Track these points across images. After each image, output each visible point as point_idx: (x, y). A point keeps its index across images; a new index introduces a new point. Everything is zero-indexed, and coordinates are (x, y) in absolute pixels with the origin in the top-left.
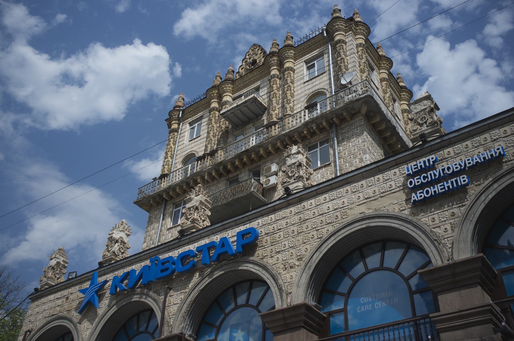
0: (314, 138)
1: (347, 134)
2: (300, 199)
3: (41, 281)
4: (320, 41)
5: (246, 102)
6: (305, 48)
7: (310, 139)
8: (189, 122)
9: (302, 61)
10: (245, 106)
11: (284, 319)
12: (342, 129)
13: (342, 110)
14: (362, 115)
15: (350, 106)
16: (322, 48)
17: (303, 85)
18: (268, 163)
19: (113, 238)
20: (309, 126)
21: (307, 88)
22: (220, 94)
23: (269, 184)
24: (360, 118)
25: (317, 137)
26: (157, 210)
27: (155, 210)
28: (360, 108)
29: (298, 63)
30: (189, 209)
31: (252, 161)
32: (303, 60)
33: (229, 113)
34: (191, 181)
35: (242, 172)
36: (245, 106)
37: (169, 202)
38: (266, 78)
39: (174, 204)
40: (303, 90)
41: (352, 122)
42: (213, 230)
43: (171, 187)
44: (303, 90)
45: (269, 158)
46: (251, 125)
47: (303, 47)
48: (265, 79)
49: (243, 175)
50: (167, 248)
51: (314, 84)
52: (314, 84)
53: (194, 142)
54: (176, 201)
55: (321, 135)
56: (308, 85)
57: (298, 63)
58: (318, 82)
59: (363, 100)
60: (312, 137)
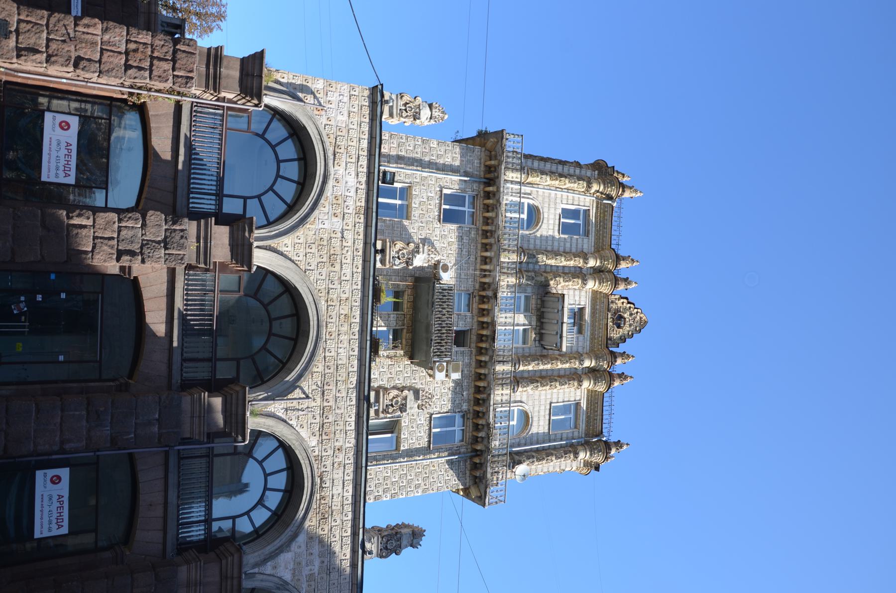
0: (471, 424)
1: (457, 468)
2: (355, 565)
3: (402, 97)
4: (593, 426)
5: (561, 337)
8: (591, 211)
9: (582, 399)
10: (557, 333)
11: (232, 578)
12: (466, 461)
13: (484, 472)
15: (484, 481)
16: (584, 428)
17: (548, 402)
18: (468, 359)
19: (416, 254)
20: (486, 428)
21: (543, 408)
22: (602, 271)
23: (436, 371)
24: (468, 484)
25: (471, 427)
26: (480, 163)
27: (480, 160)
28: (478, 487)
29: (583, 394)
30: (405, 398)
31: (481, 338)
32: (582, 401)
33: (560, 308)
34: (492, 240)
35: (473, 319)
36: (557, 333)
37: (482, 187)
38: (588, 345)
39: (477, 195)
40: (543, 402)
41: (468, 474)
42: (360, 453)
43: (498, 204)
44: (543, 402)
45: (474, 360)
46: (534, 323)
47: (599, 403)
48: (588, 342)
49: (468, 320)
50: (363, 381)
51: (542, 418)
53: (554, 224)
55: (471, 434)
56: (545, 409)
57: (583, 394)
60: (474, 423)
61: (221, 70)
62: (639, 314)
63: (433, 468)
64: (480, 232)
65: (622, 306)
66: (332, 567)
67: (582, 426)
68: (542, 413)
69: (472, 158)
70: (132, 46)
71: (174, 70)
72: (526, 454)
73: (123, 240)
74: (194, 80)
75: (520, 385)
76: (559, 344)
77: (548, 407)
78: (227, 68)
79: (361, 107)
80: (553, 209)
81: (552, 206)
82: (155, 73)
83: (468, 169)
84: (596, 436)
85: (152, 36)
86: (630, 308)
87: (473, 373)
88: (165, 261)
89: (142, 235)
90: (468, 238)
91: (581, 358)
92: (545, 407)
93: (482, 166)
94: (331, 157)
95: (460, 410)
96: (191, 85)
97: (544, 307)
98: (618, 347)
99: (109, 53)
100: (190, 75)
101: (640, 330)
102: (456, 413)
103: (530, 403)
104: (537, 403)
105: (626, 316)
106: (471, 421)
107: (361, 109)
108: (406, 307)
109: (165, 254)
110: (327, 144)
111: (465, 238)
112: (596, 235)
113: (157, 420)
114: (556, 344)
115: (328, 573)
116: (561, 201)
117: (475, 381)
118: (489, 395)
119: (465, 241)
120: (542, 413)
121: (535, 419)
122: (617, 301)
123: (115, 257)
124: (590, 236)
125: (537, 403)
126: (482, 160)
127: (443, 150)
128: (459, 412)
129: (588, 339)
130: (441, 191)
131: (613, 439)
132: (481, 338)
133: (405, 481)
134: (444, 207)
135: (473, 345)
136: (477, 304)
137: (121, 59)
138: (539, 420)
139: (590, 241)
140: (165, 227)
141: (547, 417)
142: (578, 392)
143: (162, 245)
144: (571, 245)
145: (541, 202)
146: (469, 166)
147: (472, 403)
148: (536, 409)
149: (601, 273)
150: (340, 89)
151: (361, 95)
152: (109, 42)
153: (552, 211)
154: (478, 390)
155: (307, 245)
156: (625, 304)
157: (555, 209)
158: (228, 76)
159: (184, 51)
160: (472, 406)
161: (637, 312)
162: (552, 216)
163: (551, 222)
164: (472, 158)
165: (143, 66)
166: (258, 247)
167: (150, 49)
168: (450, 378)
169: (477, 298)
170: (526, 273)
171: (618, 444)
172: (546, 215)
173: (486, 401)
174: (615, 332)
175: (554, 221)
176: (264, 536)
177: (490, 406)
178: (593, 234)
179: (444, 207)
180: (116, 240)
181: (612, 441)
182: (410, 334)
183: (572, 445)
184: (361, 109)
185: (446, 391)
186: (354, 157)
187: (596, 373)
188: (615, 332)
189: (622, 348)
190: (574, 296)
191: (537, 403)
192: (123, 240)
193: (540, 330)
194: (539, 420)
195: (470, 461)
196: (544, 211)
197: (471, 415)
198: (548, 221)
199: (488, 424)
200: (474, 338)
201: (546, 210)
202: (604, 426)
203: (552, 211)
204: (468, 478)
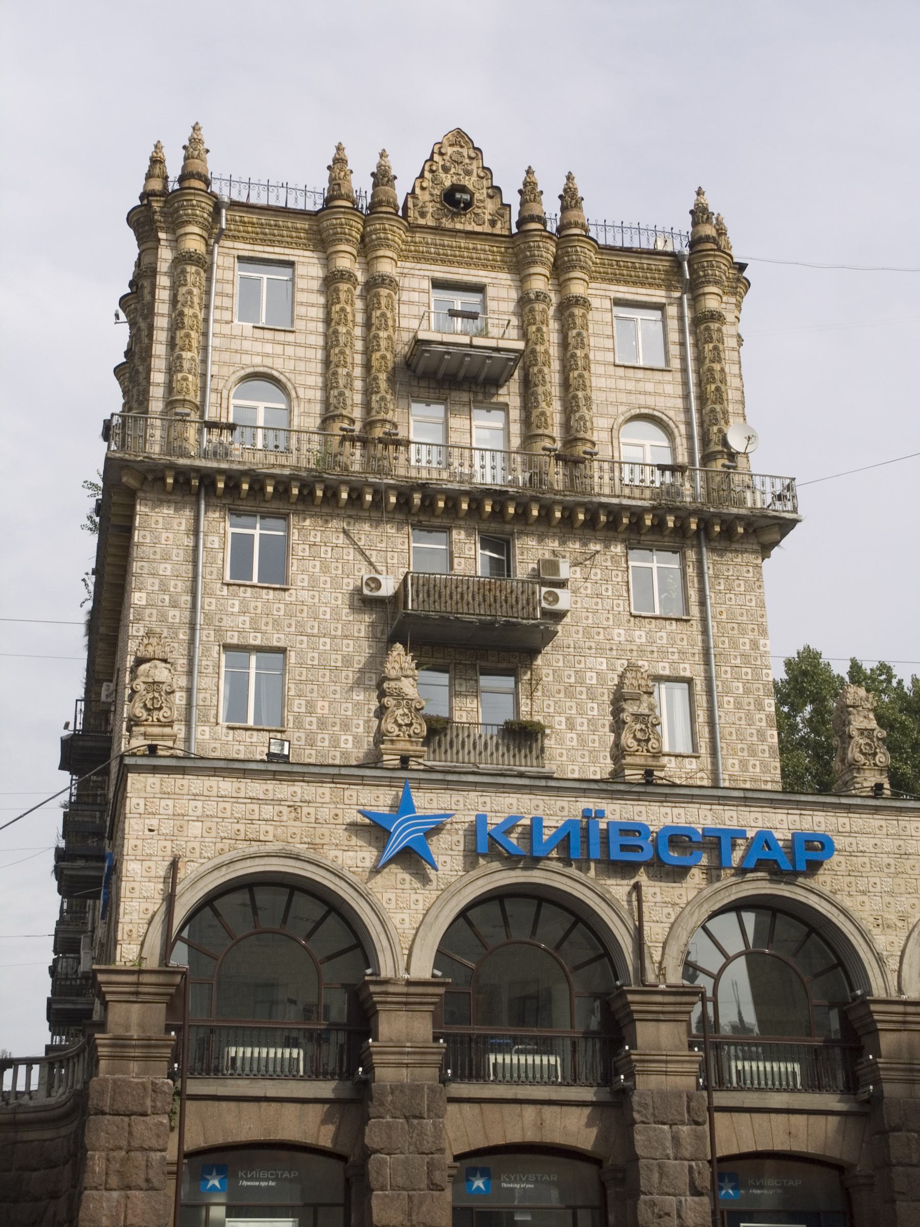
0: (649, 538)
6: (622, 264)
7: (641, 535)
8: (242, 253)
9: (608, 293)
14: (759, 543)
21: (621, 384)
25: (654, 538)
26: (169, 502)
29: (598, 292)
40: (611, 383)
44: (611, 383)
51: (641, 386)
52: (641, 386)
53: (274, 342)
54: (241, 507)
56: (625, 378)
58: (650, 387)
59: (781, 522)
61: (135, 1037)
62: (443, 151)
63: (724, 616)
64: (300, 507)
65: (427, 192)
66: (897, 851)
67: (658, 295)
68: (630, 385)
69: (160, 520)
70: (114, 1181)
71: (144, 1114)
72: (705, 426)
73: (412, 1182)
74: (157, 1081)
75: (581, 435)
76: (512, 356)
77: (621, 371)
78: (127, 1028)
79: (165, 793)
80: (244, 342)
81: (235, 344)
82: (154, 1143)
83: (183, 527)
84: (680, 266)
85: (94, 1150)
86: (432, 171)
87: (557, 530)
88: (439, 1117)
89: (402, 1153)
90: (313, 533)
91: (532, 296)
92: (621, 378)
93: (172, 497)
94: (255, 848)
95: (623, 559)
96: (166, 1087)
97: (435, 373)
98: (509, 206)
99: (130, 1216)
100: (150, 1088)
101: (475, 149)
102: (628, 568)
103: (612, 410)
104: (612, 397)
105: (448, 184)
106: (643, 538)
107: (169, 793)
108: (442, 661)
109: (429, 1118)
110: (233, 855)
111: (312, 539)
112: (289, 245)
113: (671, 1125)
114: (510, 359)
115: (906, 857)
116: (227, 323)
117: (572, 527)
118: (602, 505)
119: (318, 539)
120: (630, 385)
121: (642, 399)
122: (420, 204)
123: (436, 1193)
124: (292, 258)
125: (612, 397)
126: (163, 497)
127: (150, 581)
128: (627, 561)
129: (493, 274)
130: (228, 585)
131: (685, 225)
132: (499, 513)
133: (744, 670)
134: (255, 580)
135: (508, 528)
136: (433, 520)
137: (136, 1197)
138: (645, 393)
139: (301, 259)
140: (389, 1119)
141: (640, 374)
142: (595, 302)
143: (415, 1122)
144: (313, 305)
145: (232, 369)
146: (176, 527)
147: (610, 534)
148: (623, 397)
149: (367, 240)
150: (137, 831)
151: (143, 794)
152: (112, 1216)
153: (247, 345)
154: (591, 523)
155: (399, 886)
156: (425, 185)
157: (244, 338)
158: (142, 1026)
159: (113, 1099)
160: (616, 534)
161: (441, 154)
162: (258, 347)
163: (268, 348)
164: (160, 520)
165: (144, 1163)
166: (407, 969)
167: (115, 1154)
168: (567, 580)
169: (421, 518)
170: (374, 413)
171: (700, 214)
172: (257, 360)
173: (615, 512)
174: (480, 211)
175: (268, 341)
176: (842, 958)
177: (622, 505)
178: (287, 251)
179: (255, 580)
180: (411, 1193)
181: (690, 229)
182: (490, 653)
183: (697, 321)
184: (169, 793)
185: (588, 585)
186: (250, 806)
187: (559, 263)
188: (480, 211)
189: (512, 198)
190: (411, 303)
191: (613, 395)
192: (412, 1182)
193: (477, 384)
194: (645, 393)
195: (714, 541)
196: (248, 362)
197: (632, 536)
198: (267, 355)
199: (653, 509)
200: (494, 526)
201: (246, 359)
202: (660, 247)
203: (247, 345)
204: (745, 546)
